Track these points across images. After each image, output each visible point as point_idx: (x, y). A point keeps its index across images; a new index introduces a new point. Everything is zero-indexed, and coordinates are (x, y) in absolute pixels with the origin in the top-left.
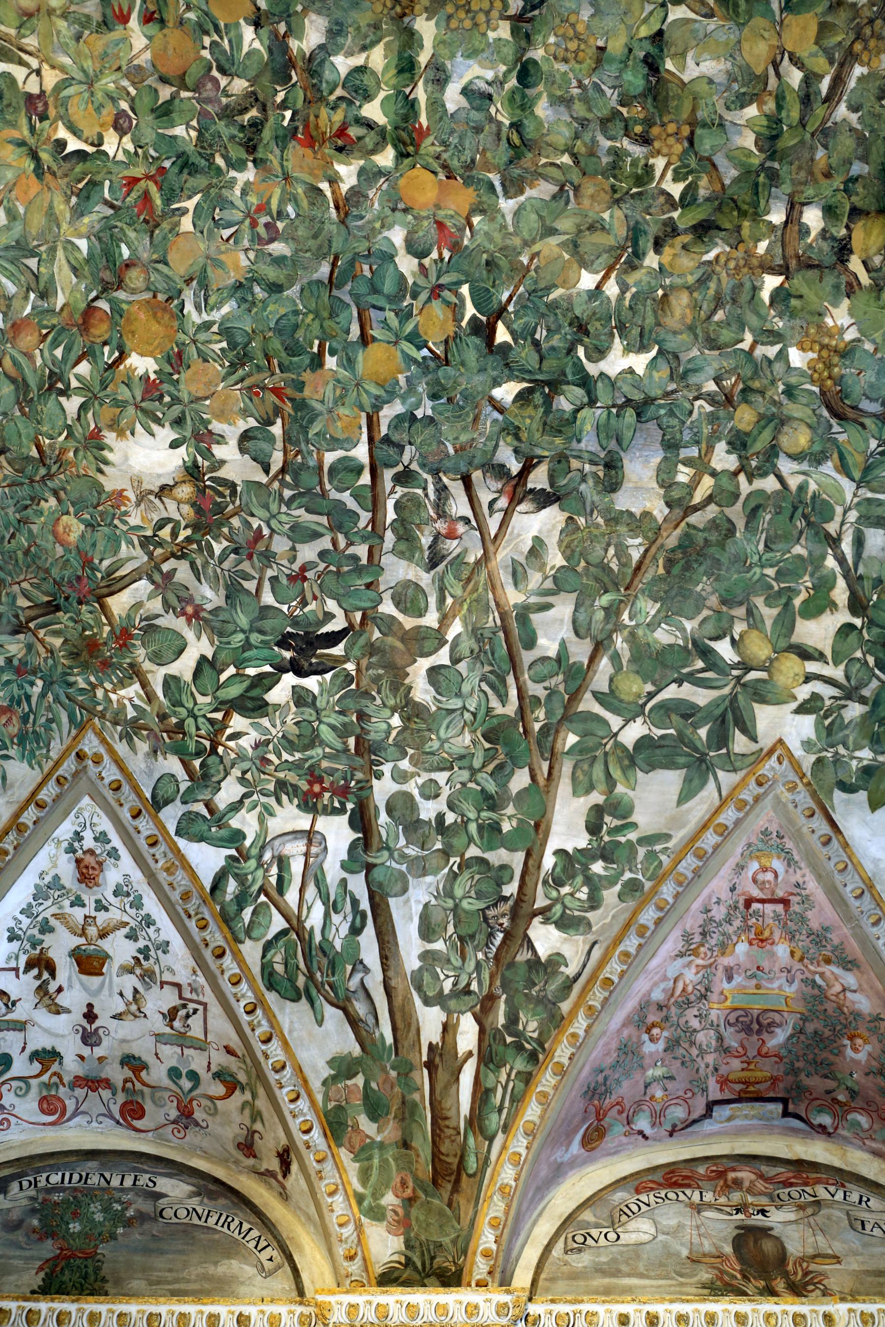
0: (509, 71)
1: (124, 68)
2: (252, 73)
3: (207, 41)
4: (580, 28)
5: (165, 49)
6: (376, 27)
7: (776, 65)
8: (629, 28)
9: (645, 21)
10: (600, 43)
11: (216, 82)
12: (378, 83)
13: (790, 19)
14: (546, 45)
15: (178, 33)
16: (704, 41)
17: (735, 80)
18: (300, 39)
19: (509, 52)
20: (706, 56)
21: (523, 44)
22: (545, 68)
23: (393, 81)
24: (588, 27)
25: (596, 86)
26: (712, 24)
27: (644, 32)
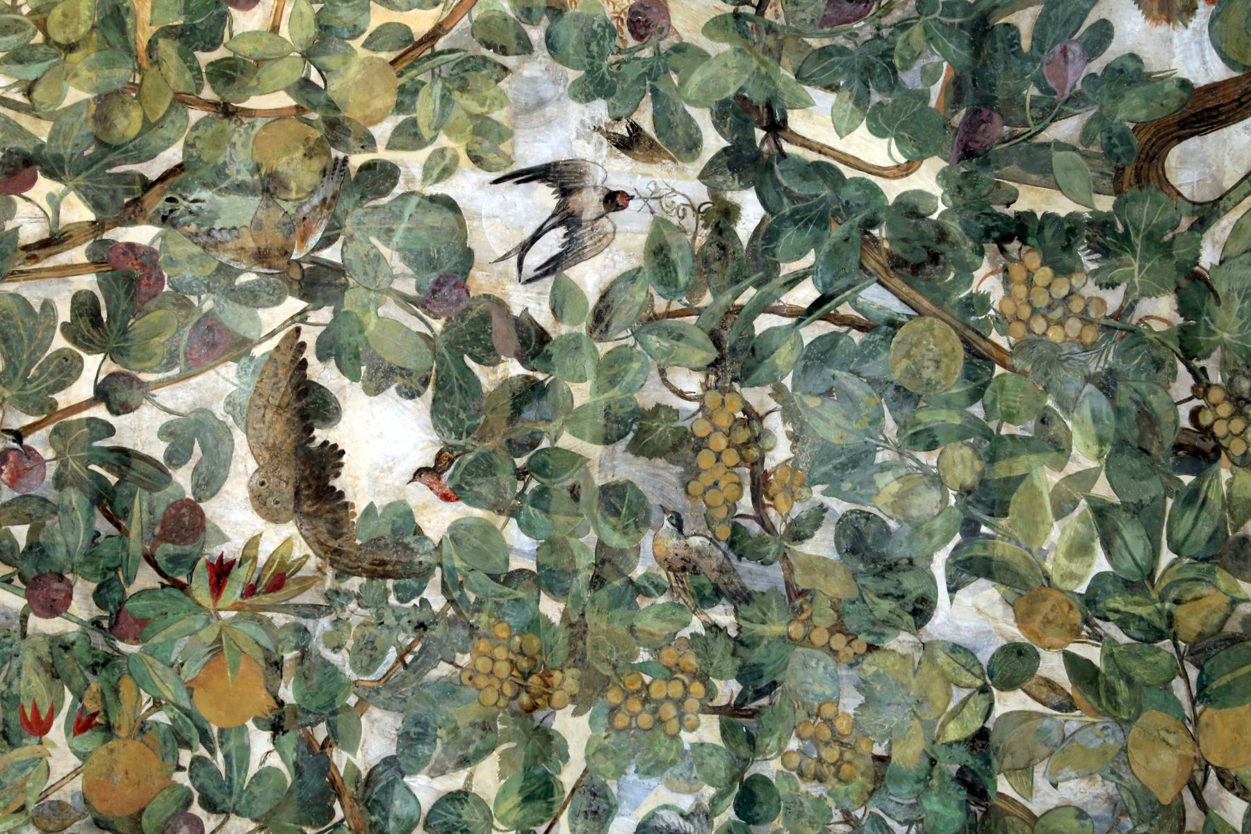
0: (721, 796)
1: (32, 807)
2: (262, 808)
3: (185, 757)
4: (842, 725)
5: (109, 774)
6: (486, 727)
7: (1197, 791)
8: (928, 726)
9: (955, 714)
10: (879, 750)
11: (197, 824)
12: (488, 818)
13: (1209, 714)
14: (784, 755)
15: (134, 746)
16: (1061, 750)
17: (1126, 812)
18: (352, 749)
19: (719, 765)
20: (1067, 771)
21: (744, 751)
22: (783, 789)
23: (516, 815)
24: (855, 724)
25: (877, 821)
26: (1073, 722)
27: (954, 732)
